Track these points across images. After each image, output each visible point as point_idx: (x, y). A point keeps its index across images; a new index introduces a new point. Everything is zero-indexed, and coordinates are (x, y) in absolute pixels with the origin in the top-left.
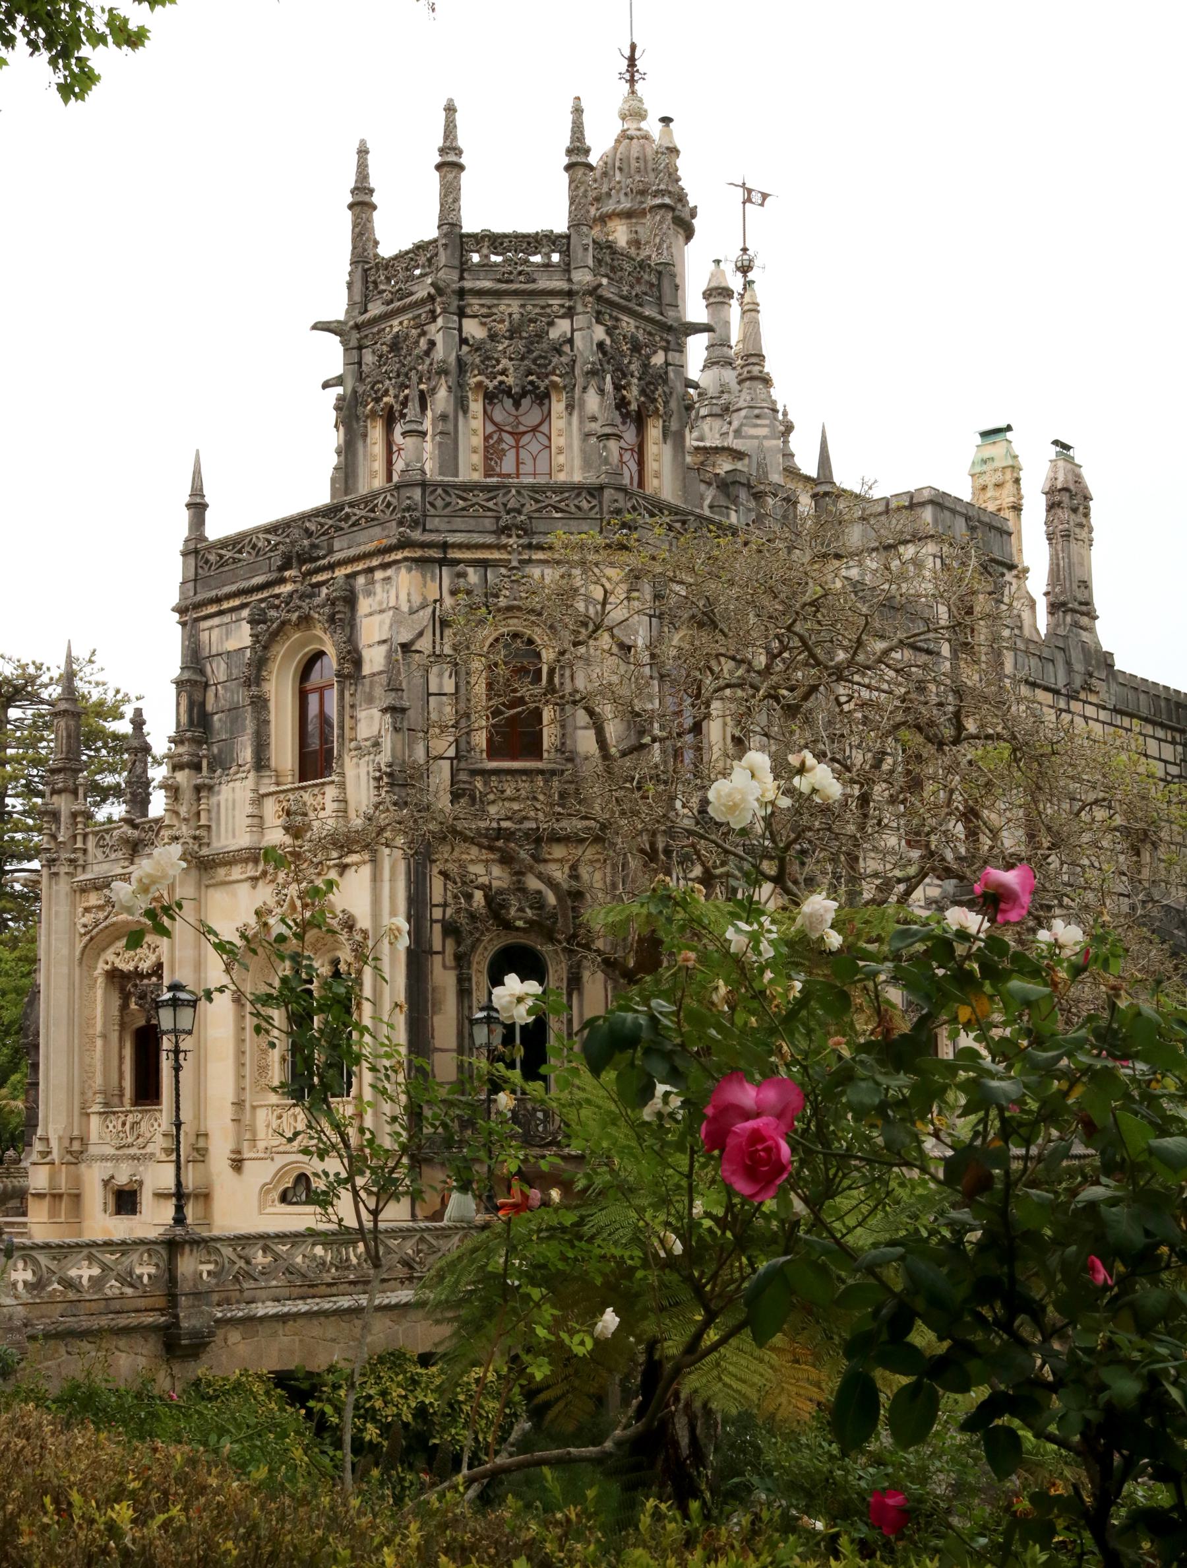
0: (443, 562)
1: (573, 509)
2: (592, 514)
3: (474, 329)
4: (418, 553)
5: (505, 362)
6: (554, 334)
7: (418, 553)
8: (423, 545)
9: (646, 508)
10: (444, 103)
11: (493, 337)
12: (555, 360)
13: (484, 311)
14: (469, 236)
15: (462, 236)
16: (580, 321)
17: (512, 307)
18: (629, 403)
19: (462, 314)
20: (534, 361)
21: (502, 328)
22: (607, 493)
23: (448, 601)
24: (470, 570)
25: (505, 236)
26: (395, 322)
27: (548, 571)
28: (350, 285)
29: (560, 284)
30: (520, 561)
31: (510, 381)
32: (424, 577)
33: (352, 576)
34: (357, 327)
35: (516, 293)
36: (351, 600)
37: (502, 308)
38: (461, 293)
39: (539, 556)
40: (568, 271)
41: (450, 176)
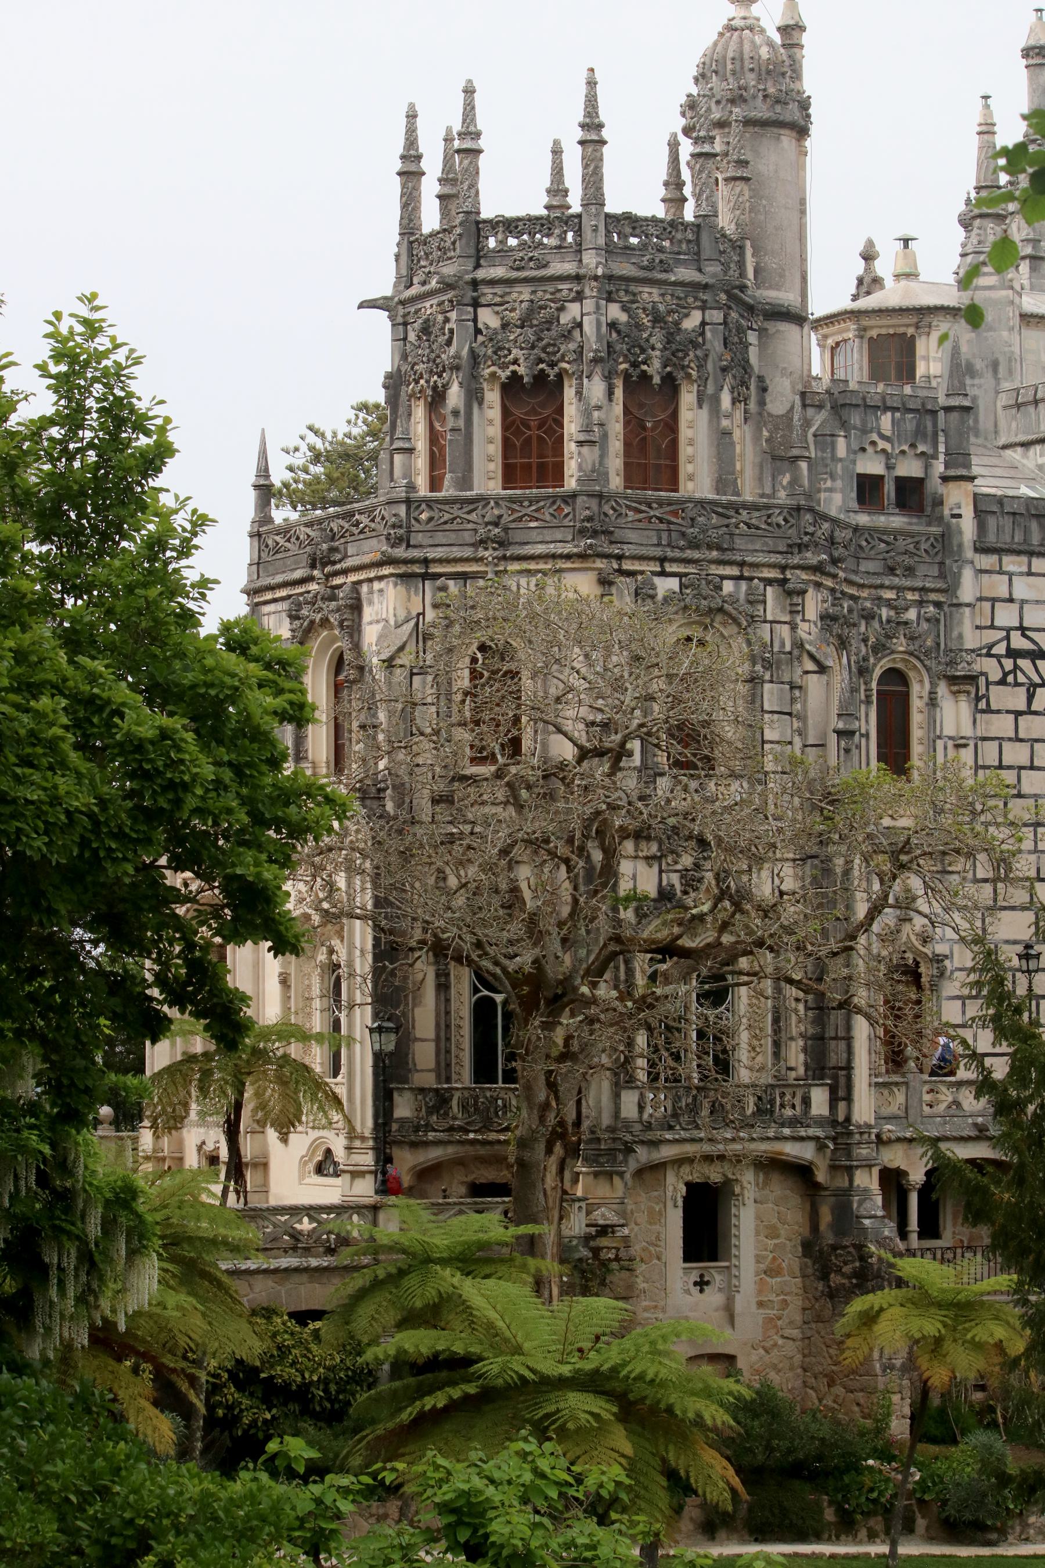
0: (425, 577)
1: (548, 517)
2: (566, 522)
3: (488, 318)
4: (402, 569)
5: (516, 352)
6: (565, 319)
7: (402, 569)
8: (406, 562)
9: (628, 507)
10: (463, 84)
11: (505, 326)
12: (563, 348)
13: (498, 299)
14: (485, 221)
15: (478, 223)
16: (589, 305)
17: (524, 293)
18: (651, 377)
19: (476, 304)
20: (544, 349)
21: (515, 315)
22: (580, 500)
23: (430, 615)
24: (451, 583)
25: (519, 219)
26: (428, 305)
27: (523, 582)
28: (397, 257)
29: (568, 267)
30: (497, 573)
31: (521, 370)
32: (408, 591)
33: (360, 582)
34: (402, 303)
35: (526, 280)
36: (356, 607)
37: (514, 295)
38: (475, 284)
39: (515, 566)
40: (580, 251)
41: (466, 162)
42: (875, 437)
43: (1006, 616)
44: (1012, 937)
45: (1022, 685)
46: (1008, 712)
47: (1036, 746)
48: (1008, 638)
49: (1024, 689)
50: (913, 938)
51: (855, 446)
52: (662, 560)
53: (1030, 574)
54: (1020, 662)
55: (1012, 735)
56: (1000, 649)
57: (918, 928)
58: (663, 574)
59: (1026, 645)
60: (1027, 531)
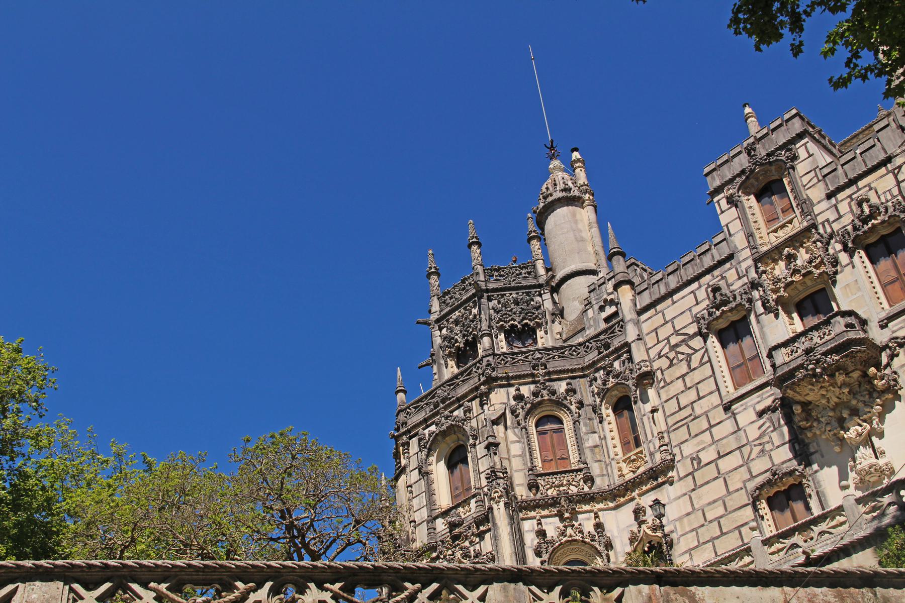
42: (605, 296)
43: (664, 333)
44: (711, 500)
45: (681, 360)
46: (677, 379)
47: (699, 386)
48: (669, 342)
49: (684, 362)
50: (649, 532)
51: (596, 307)
52: (425, 420)
53: (674, 303)
54: (678, 349)
55: (683, 388)
56: (666, 350)
57: (650, 524)
58: (428, 427)
59: (681, 338)
60: (667, 284)
